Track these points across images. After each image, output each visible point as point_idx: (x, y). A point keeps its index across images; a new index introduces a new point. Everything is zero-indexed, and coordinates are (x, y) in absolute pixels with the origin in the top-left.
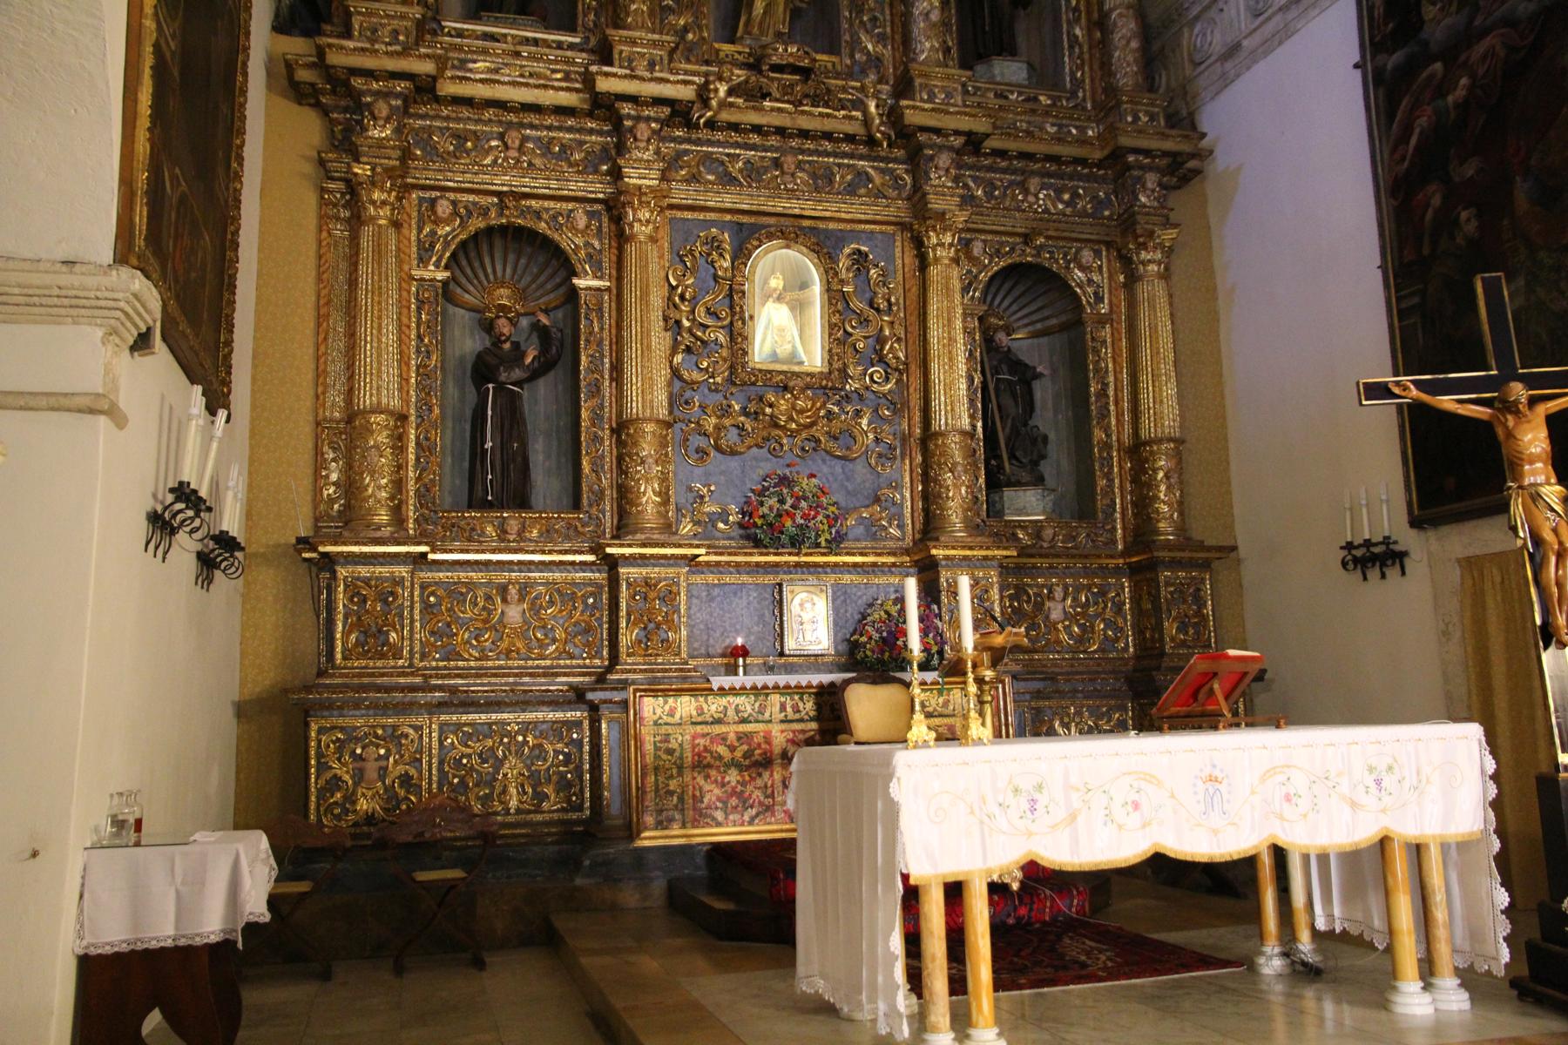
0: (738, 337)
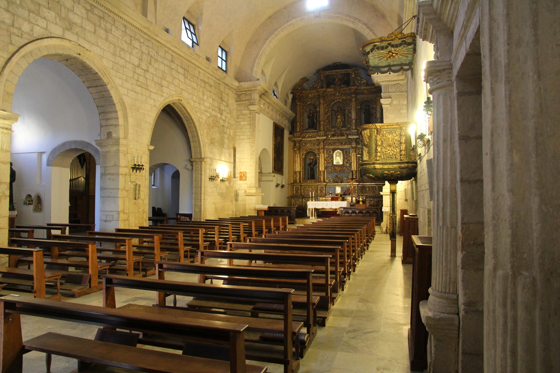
0: (333, 161)
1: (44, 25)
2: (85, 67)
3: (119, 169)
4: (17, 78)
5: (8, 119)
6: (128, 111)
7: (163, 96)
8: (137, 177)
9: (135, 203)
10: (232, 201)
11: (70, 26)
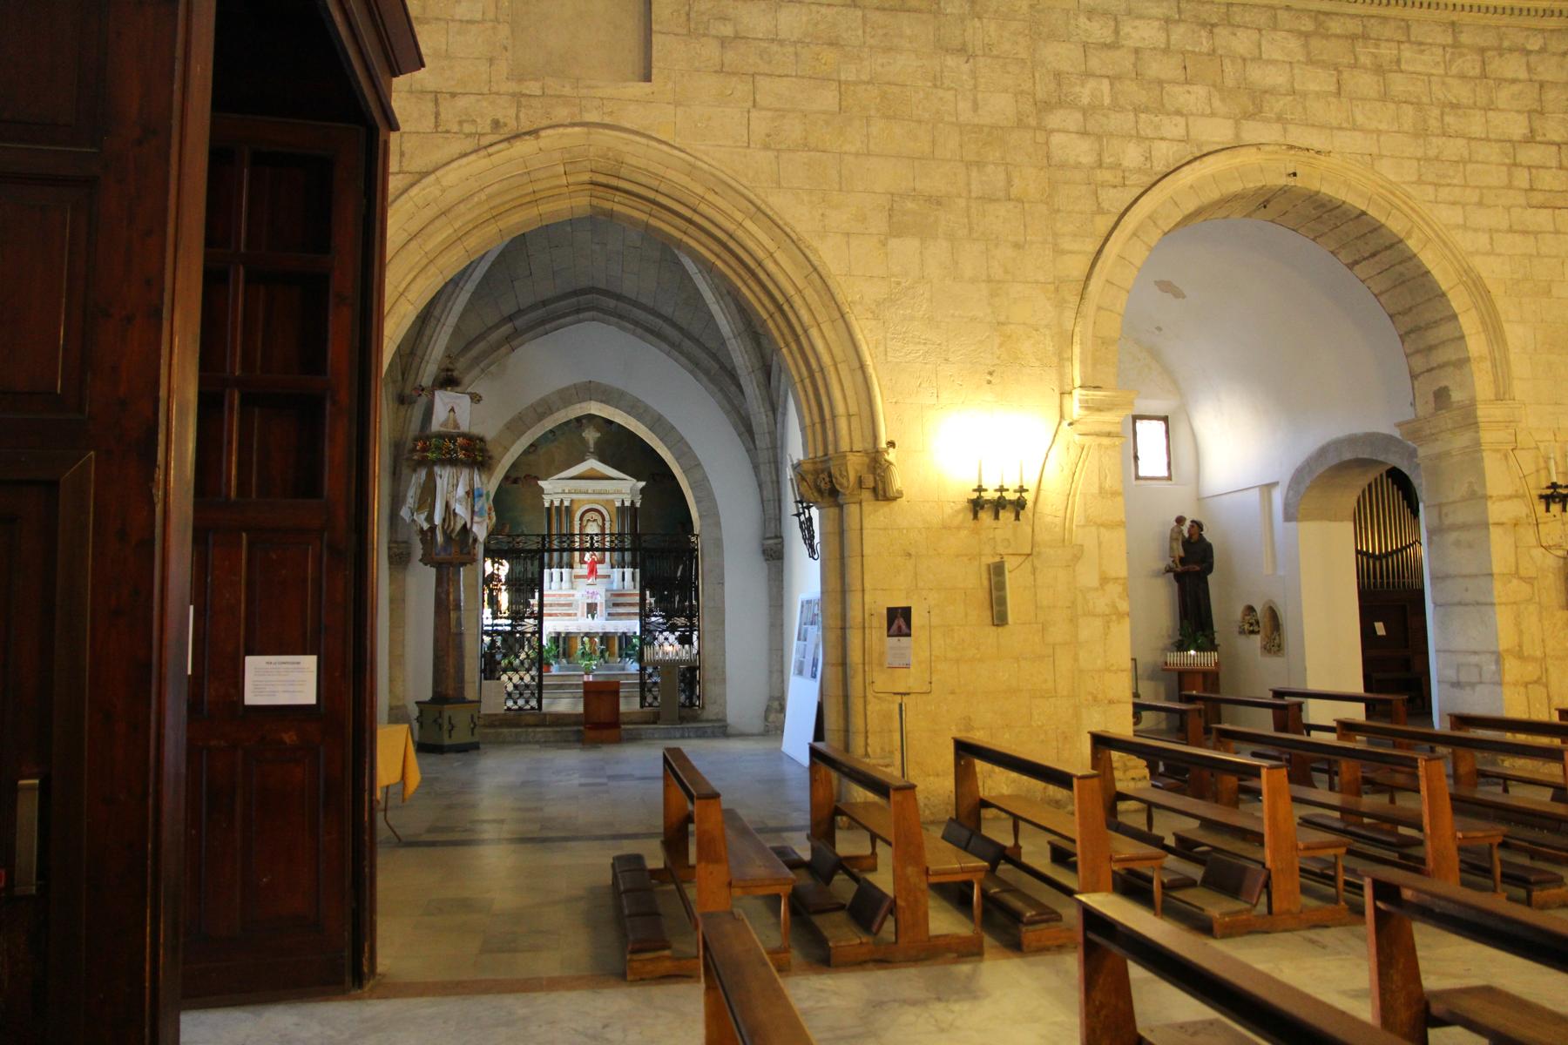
1: (1180, 132)
2: (1323, 205)
3: (1485, 511)
4: (1124, 296)
5: (1109, 409)
6: (1502, 304)
11: (1254, 103)
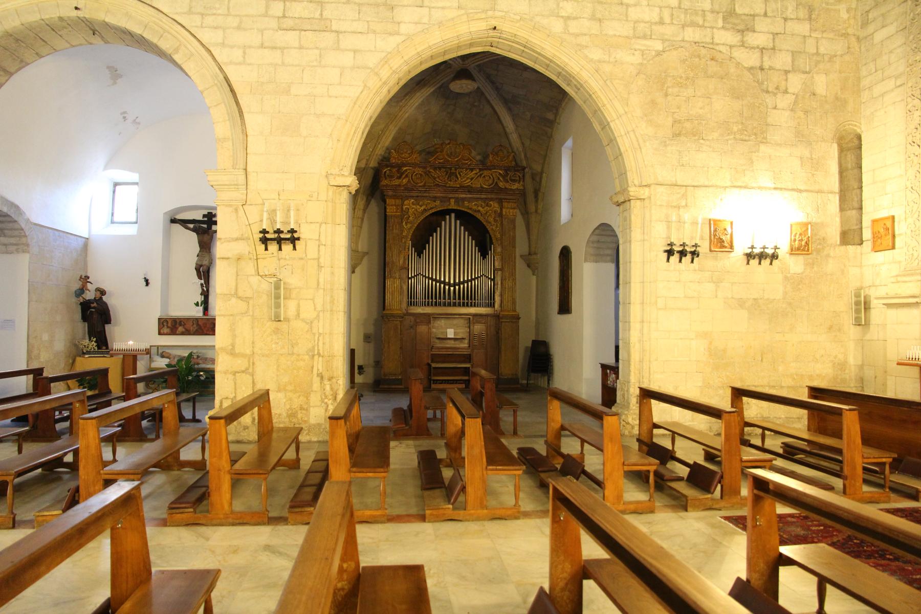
7: (398, 34)
8: (283, 262)
9: (277, 331)
10: (833, 329)
